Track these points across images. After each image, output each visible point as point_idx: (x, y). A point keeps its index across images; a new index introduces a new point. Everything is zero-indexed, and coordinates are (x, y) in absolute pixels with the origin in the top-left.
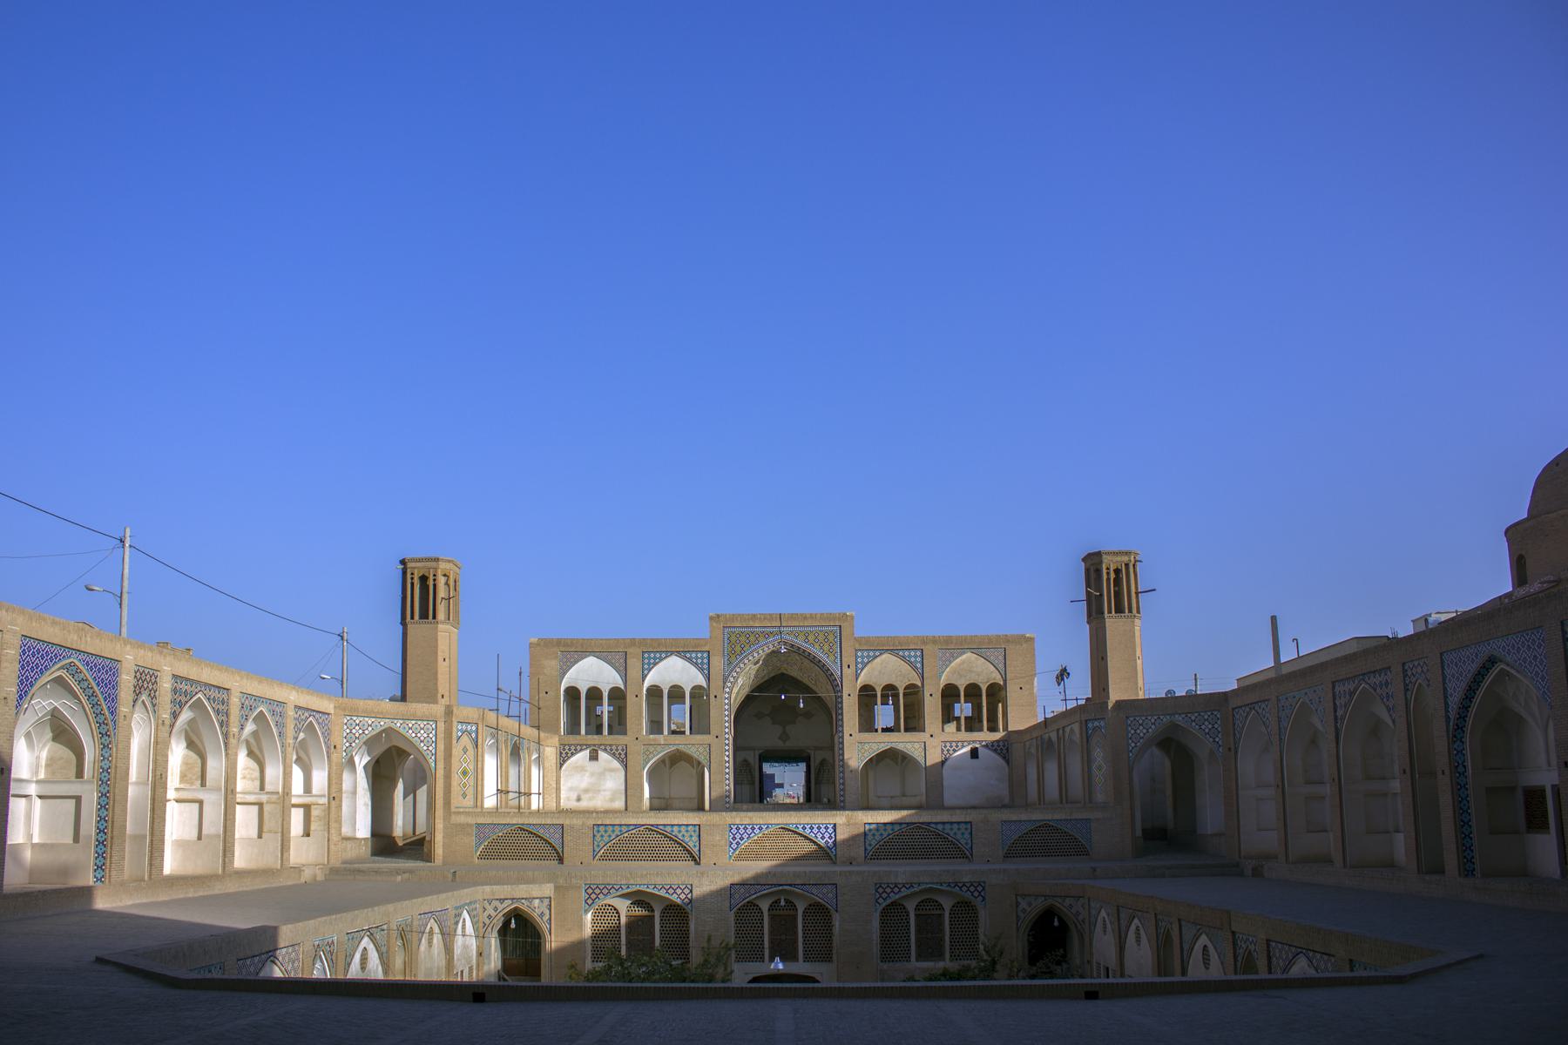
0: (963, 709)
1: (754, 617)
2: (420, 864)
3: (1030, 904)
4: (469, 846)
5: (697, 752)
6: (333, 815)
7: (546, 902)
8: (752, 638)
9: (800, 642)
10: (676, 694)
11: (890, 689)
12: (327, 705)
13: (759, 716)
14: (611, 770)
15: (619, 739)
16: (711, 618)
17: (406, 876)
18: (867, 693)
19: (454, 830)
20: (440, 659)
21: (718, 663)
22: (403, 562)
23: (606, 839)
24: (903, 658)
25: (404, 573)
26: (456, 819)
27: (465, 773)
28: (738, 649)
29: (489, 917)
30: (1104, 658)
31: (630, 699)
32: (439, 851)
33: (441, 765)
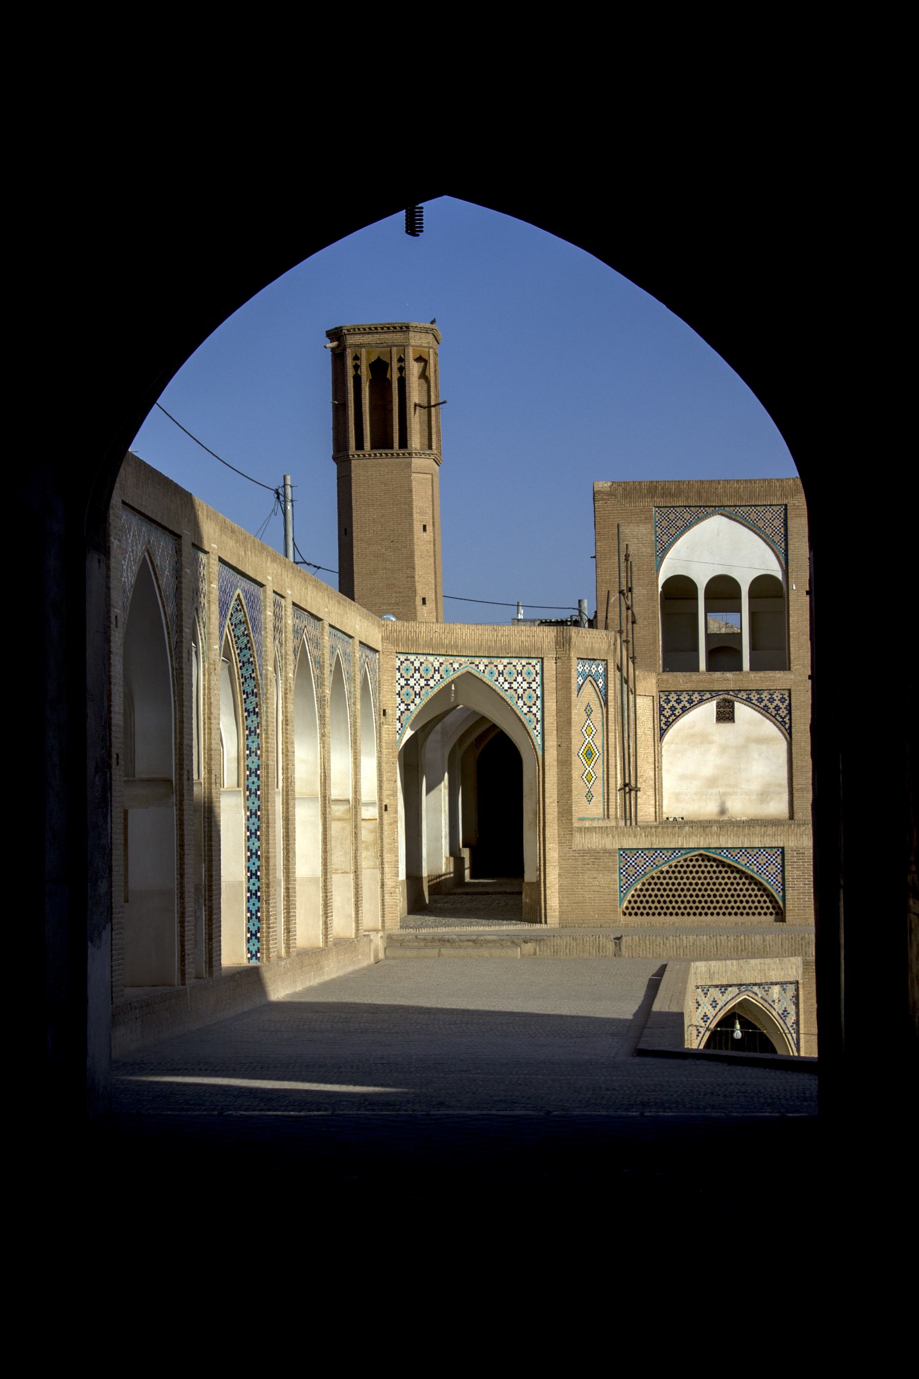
2: (526, 927)
4: (607, 888)
6: (386, 840)
7: (791, 989)
12: (375, 638)
14: (763, 741)
17: (529, 947)
19: (581, 862)
20: (418, 527)
22: (336, 335)
25: (338, 357)
26: (581, 841)
27: (589, 754)
29: (705, 1018)
32: (553, 900)
33: (552, 741)
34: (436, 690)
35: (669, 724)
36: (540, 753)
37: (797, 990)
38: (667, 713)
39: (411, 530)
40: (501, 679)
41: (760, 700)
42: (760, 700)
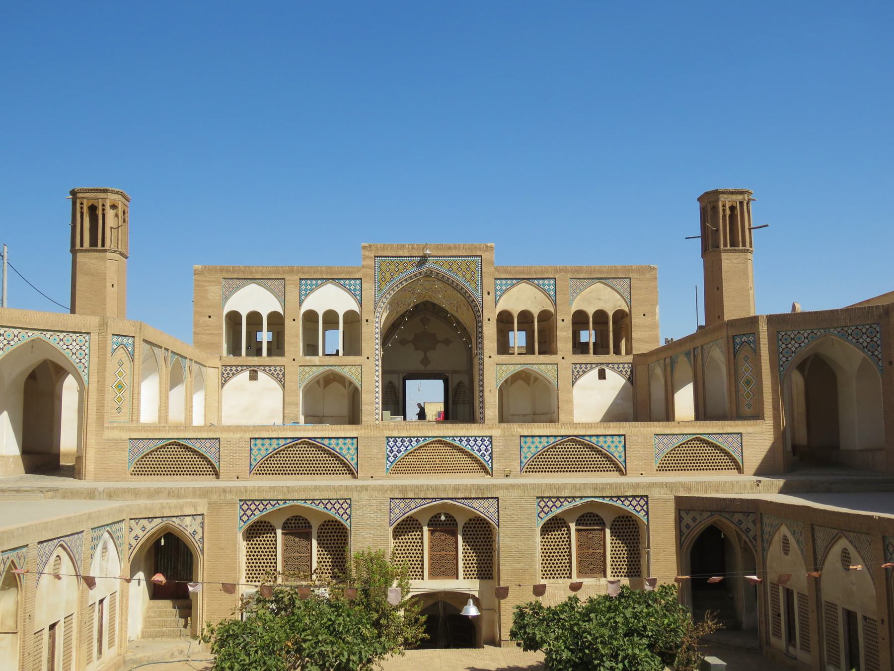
0: (588, 336)
1: (403, 247)
3: (694, 519)
4: (123, 458)
5: (348, 373)
8: (401, 267)
9: (444, 270)
10: (331, 319)
11: (525, 318)
13: (403, 342)
15: (276, 360)
16: (364, 248)
18: (504, 320)
21: (369, 289)
23: (263, 453)
24: (538, 287)
26: (109, 434)
27: (120, 387)
28: (388, 276)
29: (136, 538)
30: (719, 288)
31: (288, 322)
34: (14, 347)
35: (226, 381)
36: (86, 385)
37: (203, 519)
38: (225, 376)
39: (105, 287)
40: (61, 343)
41: (270, 370)
42: (270, 370)
